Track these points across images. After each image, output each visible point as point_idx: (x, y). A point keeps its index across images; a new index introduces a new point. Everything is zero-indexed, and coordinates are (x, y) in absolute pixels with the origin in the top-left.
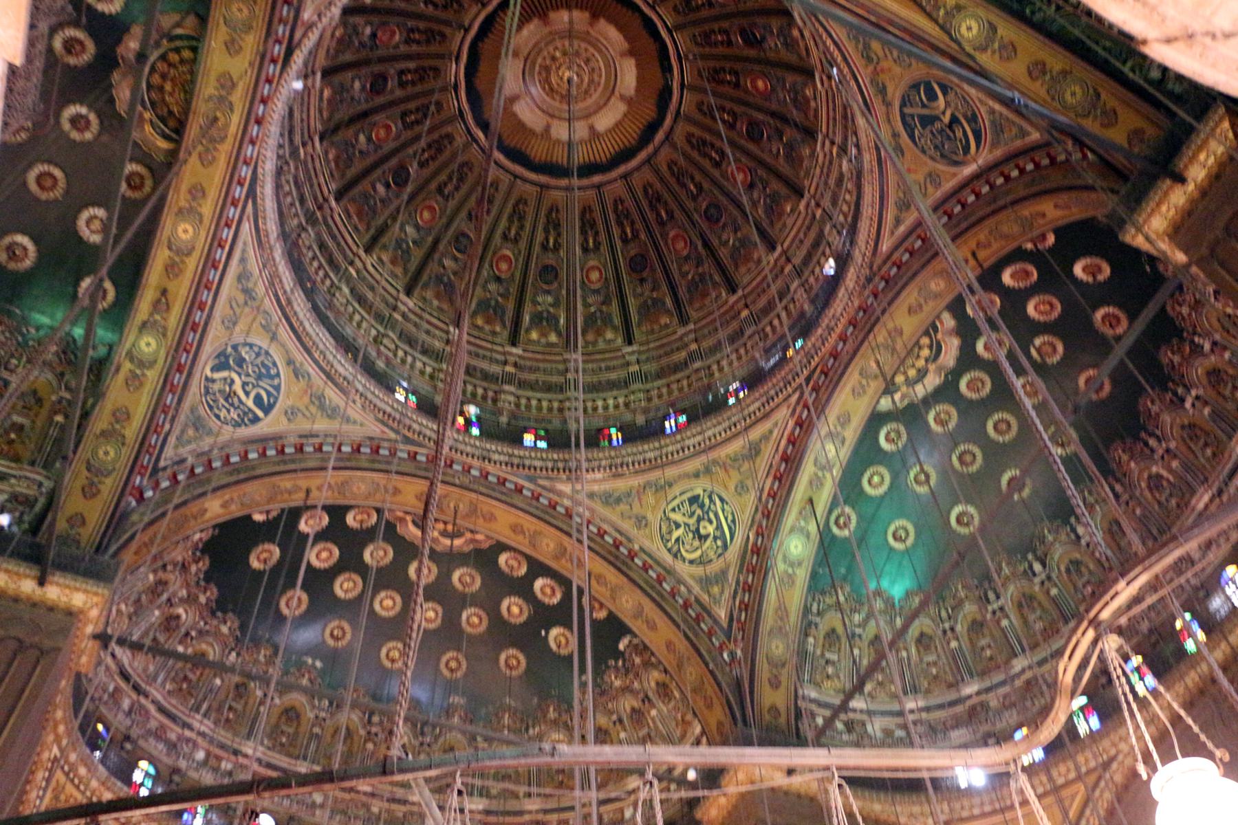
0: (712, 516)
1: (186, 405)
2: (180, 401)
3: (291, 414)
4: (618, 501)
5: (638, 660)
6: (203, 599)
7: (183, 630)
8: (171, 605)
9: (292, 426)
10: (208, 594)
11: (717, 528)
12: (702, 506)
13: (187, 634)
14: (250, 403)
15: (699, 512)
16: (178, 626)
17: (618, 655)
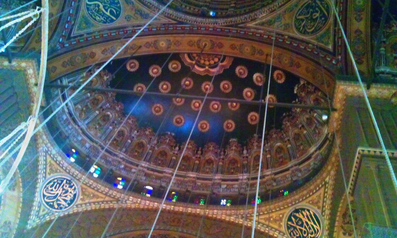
0: (317, 9)
1: (81, 13)
2: (76, 13)
3: (128, 18)
4: (274, 22)
5: (303, 94)
6: (118, 108)
7: (111, 121)
8: (103, 110)
9: (130, 23)
10: (119, 107)
11: (320, 13)
12: (312, 7)
13: (113, 122)
14: (108, 13)
15: (311, 10)
16: (108, 120)
17: (296, 96)
